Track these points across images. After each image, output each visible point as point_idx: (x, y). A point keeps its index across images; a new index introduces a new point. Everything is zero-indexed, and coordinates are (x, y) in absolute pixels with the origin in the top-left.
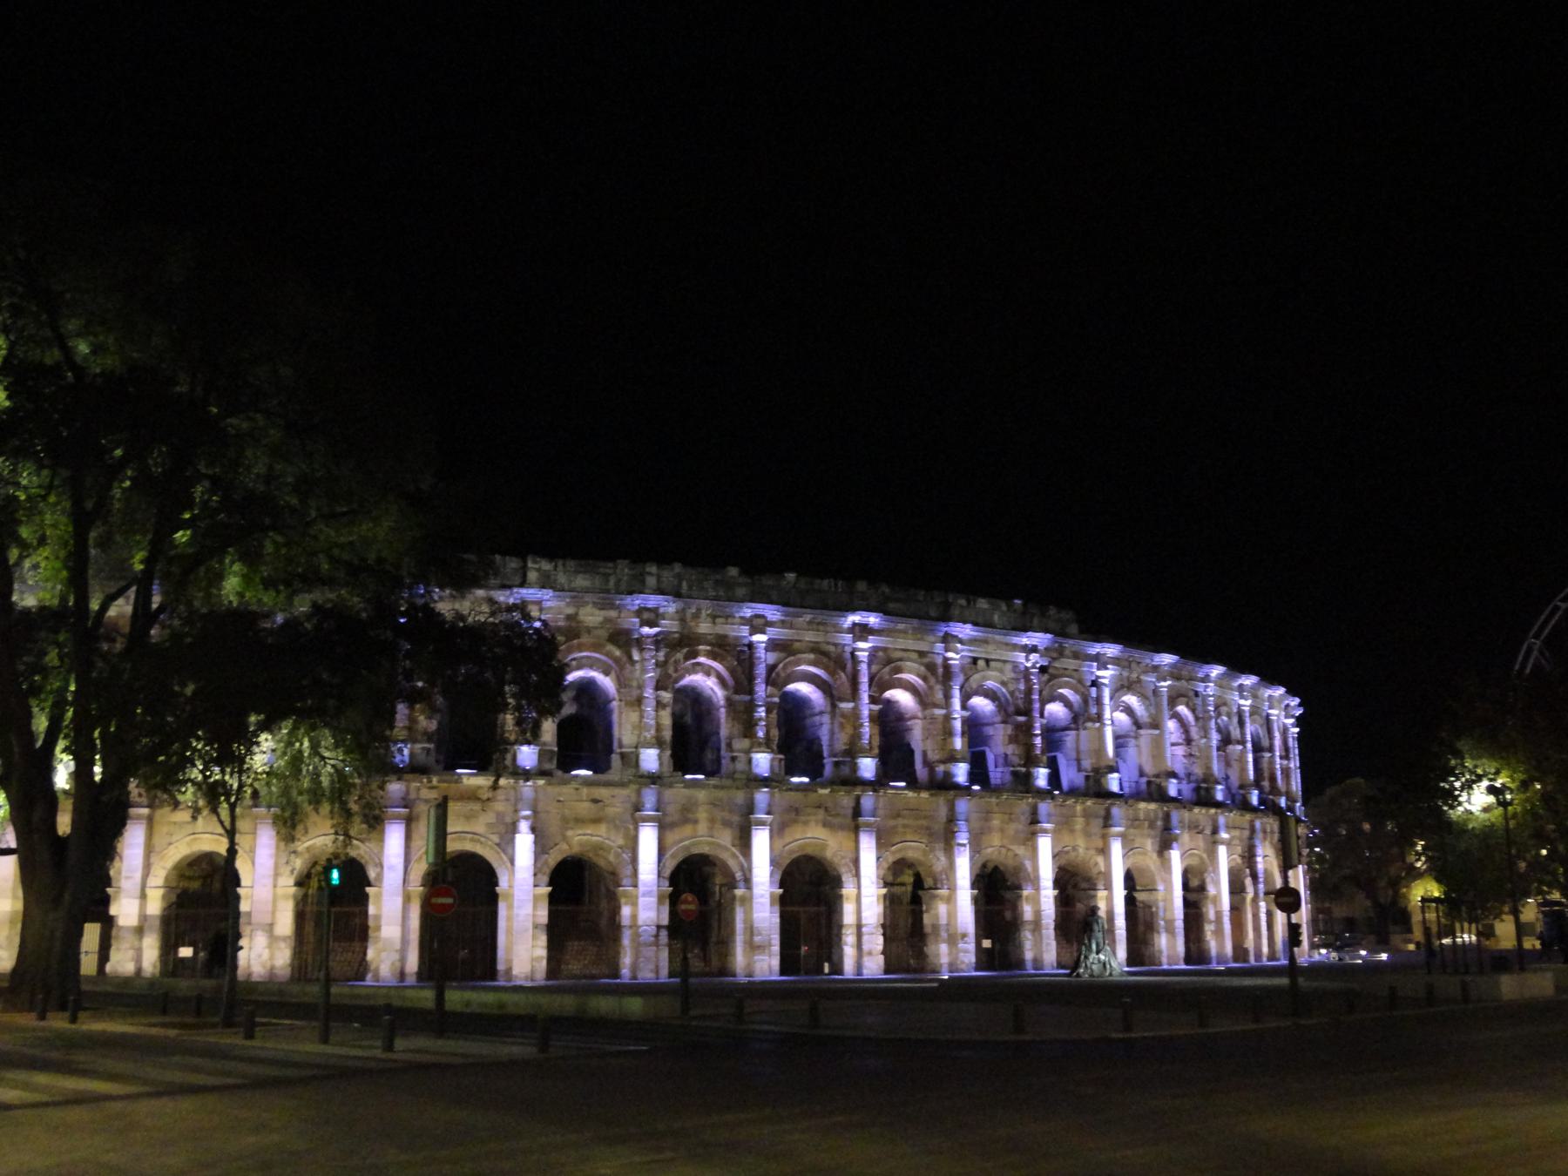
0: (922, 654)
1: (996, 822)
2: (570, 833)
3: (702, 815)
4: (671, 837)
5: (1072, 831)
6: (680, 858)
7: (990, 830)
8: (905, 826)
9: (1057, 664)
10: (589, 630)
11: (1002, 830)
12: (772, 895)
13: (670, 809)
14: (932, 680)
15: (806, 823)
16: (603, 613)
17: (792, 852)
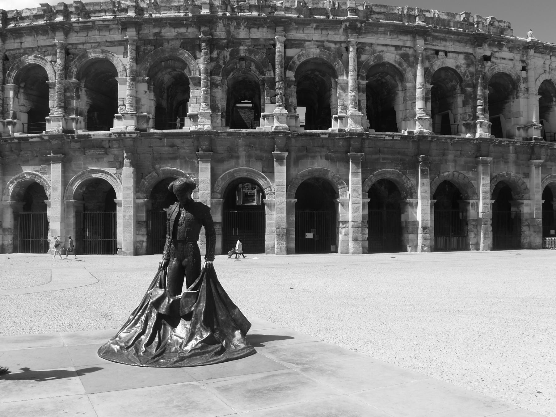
0: (397, 47)
1: (450, 157)
2: (157, 166)
3: (242, 153)
4: (221, 167)
5: (506, 162)
6: (229, 180)
7: (446, 161)
8: (384, 159)
9: (497, 55)
10: (168, 41)
11: (455, 161)
12: (288, 204)
13: (220, 149)
14: (405, 65)
15: (314, 157)
16: (177, 30)
17: (303, 175)
